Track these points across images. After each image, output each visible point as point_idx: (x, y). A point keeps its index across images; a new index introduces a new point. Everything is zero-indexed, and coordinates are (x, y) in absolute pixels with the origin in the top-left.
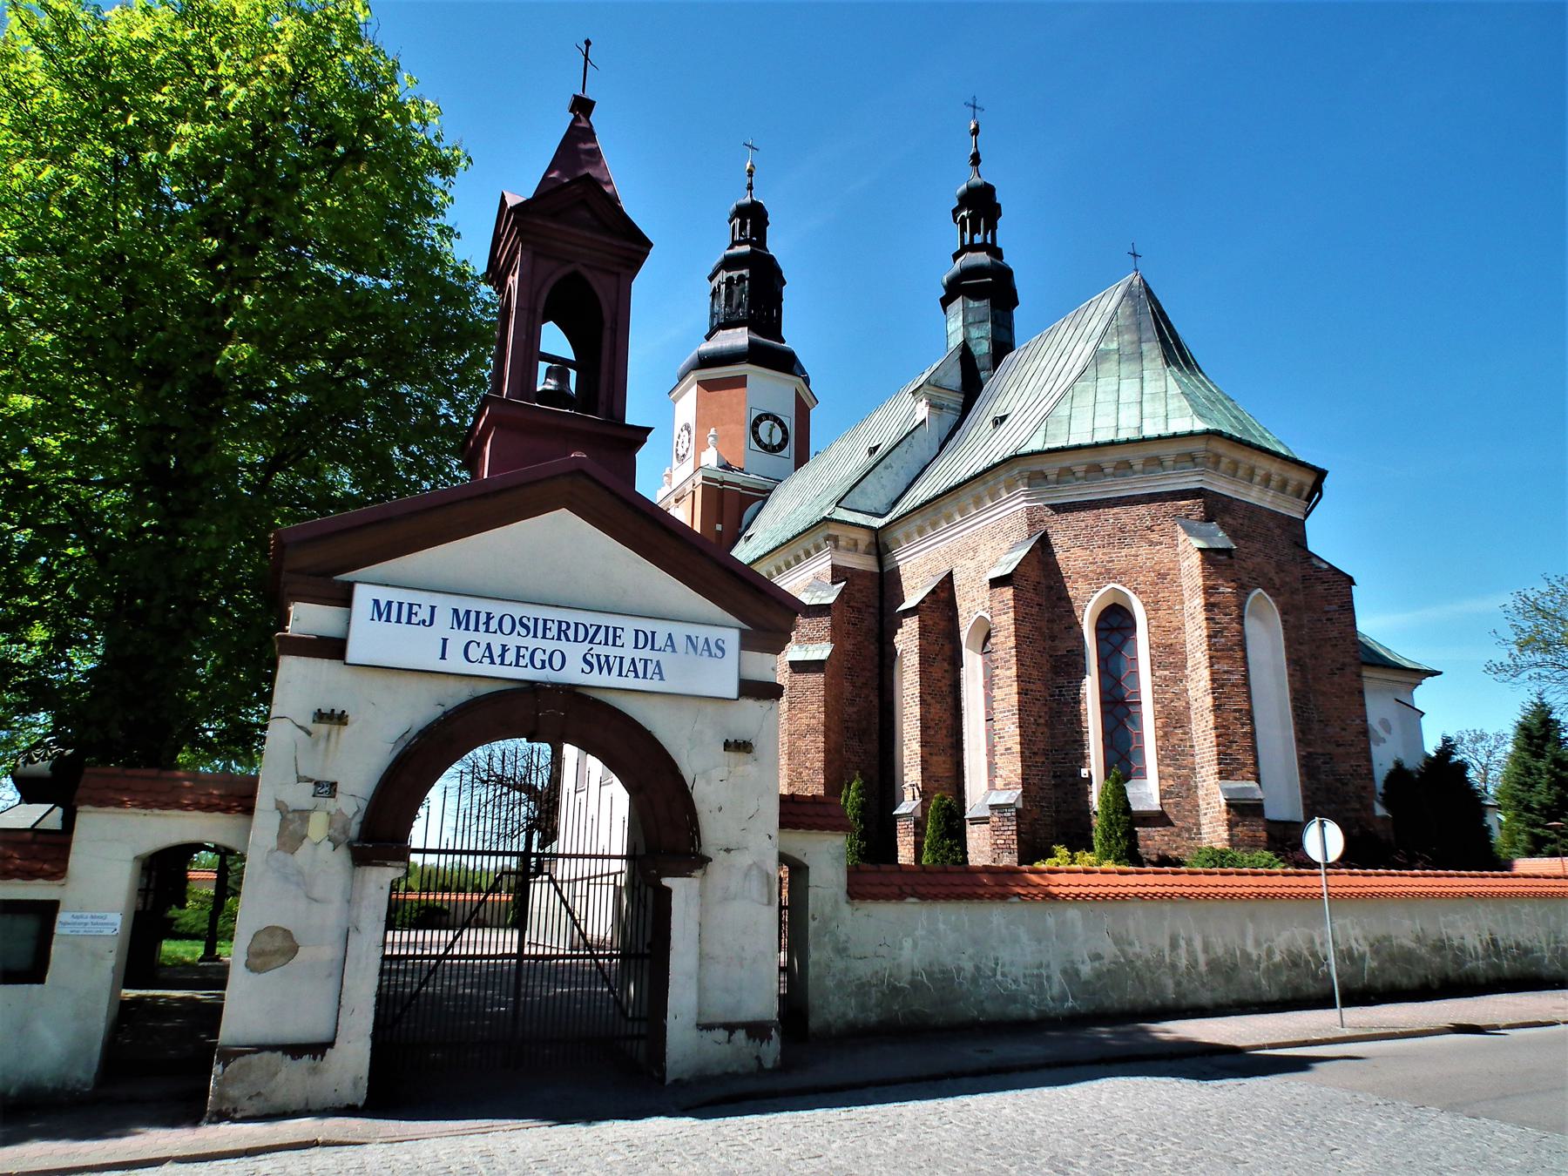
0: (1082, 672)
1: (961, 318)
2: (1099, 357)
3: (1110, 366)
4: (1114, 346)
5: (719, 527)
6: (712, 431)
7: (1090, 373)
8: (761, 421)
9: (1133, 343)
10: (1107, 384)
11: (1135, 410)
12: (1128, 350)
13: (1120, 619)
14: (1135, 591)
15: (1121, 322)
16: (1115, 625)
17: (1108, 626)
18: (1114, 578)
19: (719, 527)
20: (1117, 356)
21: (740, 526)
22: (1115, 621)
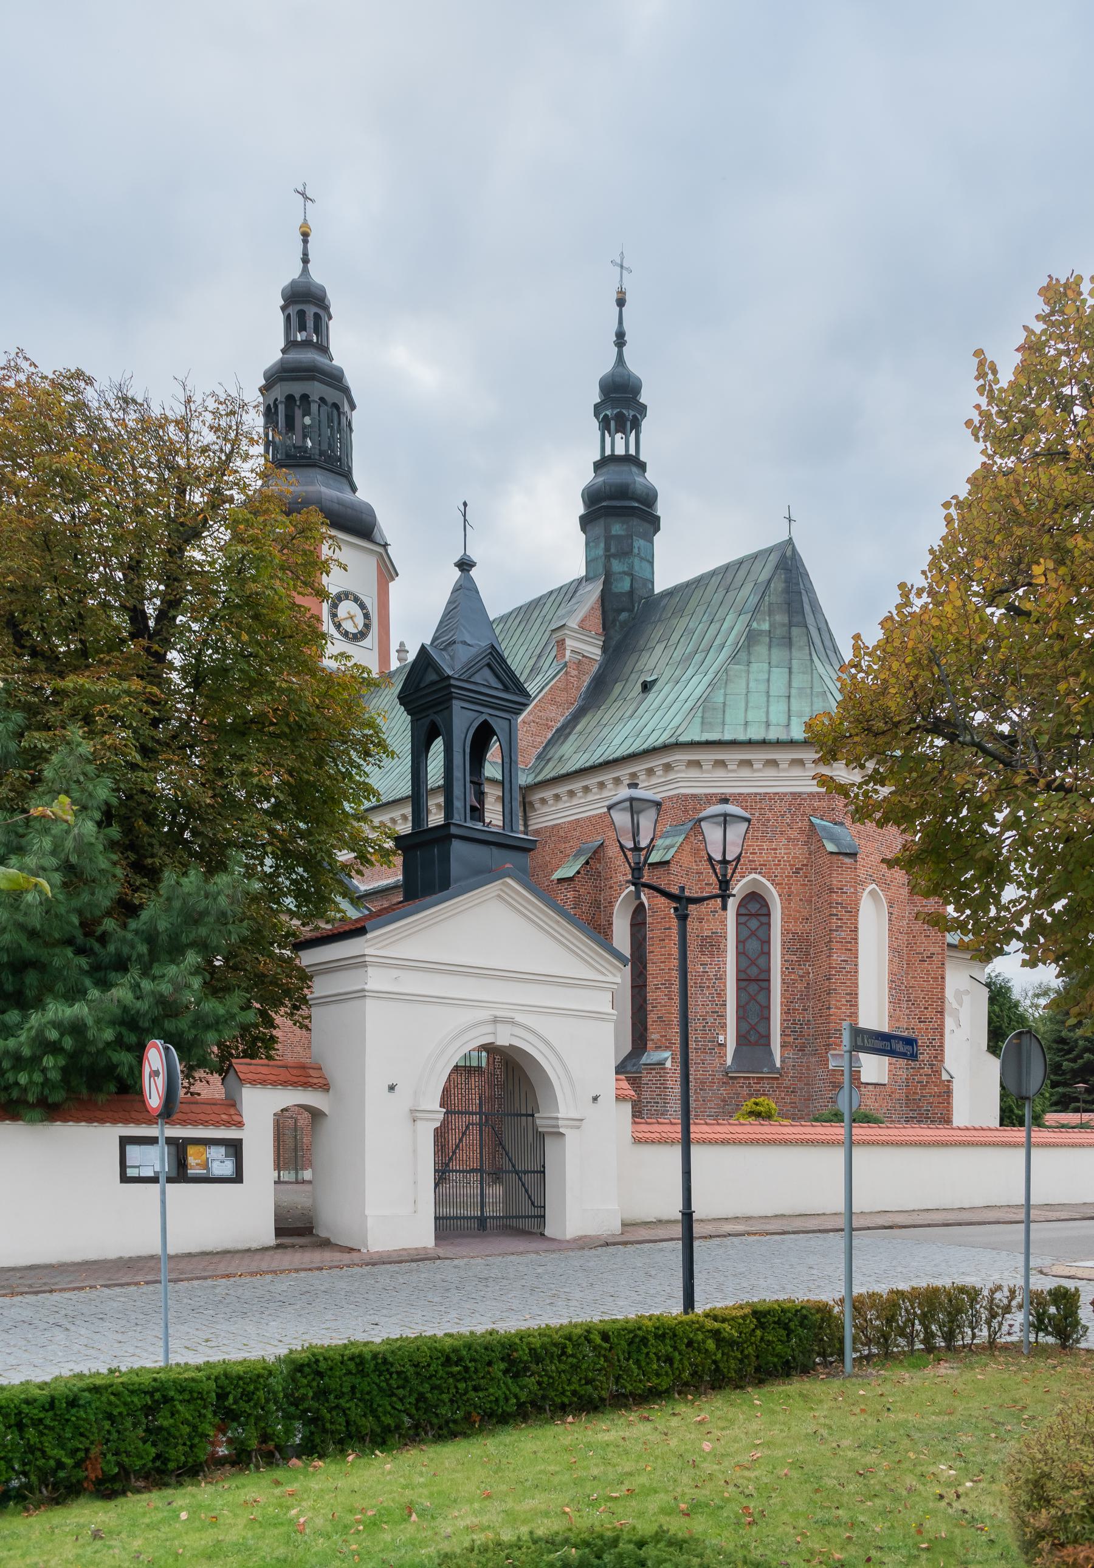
0: (722, 952)
1: (602, 545)
2: (751, 638)
3: (761, 650)
4: (766, 626)
7: (743, 655)
8: (340, 600)
9: (784, 625)
10: (758, 668)
11: (783, 706)
12: (779, 632)
13: (758, 906)
14: (773, 882)
15: (773, 599)
16: (753, 912)
17: (746, 912)
18: (754, 870)
20: (767, 639)
22: (754, 907)
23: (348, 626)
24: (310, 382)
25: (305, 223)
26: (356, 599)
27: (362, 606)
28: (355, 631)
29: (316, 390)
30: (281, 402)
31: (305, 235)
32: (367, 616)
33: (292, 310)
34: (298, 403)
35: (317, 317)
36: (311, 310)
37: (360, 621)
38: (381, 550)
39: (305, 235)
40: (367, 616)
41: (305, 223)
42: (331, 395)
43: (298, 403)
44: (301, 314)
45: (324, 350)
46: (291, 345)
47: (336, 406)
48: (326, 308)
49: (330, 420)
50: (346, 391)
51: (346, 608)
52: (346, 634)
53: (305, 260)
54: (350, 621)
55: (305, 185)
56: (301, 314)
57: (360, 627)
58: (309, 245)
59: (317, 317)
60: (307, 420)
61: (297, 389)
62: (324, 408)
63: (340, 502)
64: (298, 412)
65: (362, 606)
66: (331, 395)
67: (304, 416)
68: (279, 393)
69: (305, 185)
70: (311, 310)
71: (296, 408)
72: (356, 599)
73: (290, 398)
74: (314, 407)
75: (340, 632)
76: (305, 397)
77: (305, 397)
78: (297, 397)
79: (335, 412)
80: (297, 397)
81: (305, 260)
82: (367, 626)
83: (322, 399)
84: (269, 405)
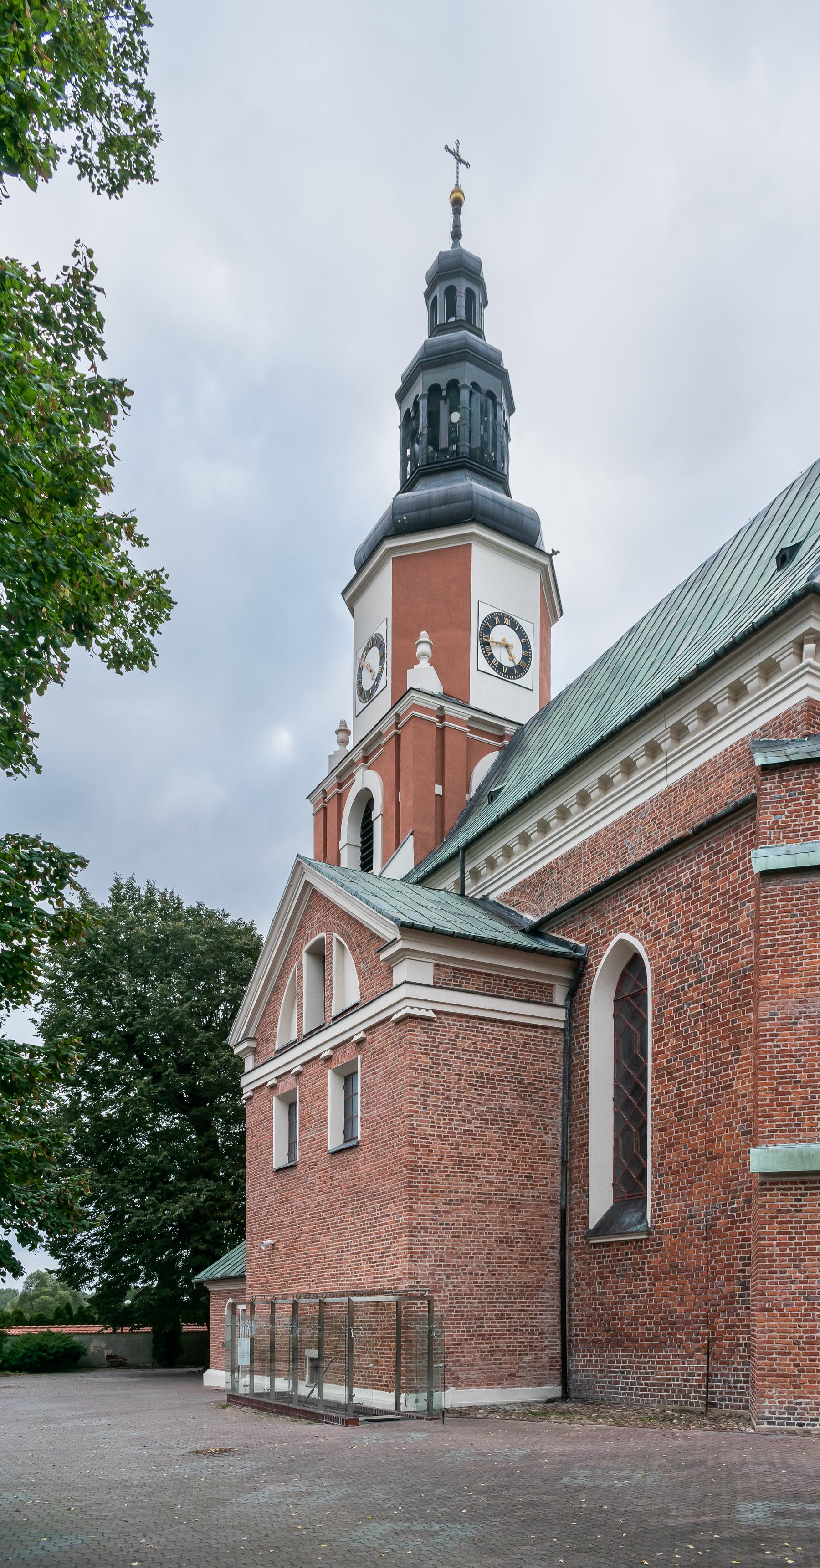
5: (438, 790)
6: (424, 635)
8: (494, 624)
19: (438, 790)
21: (468, 790)
23: (501, 656)
24: (461, 364)
25: (458, 189)
26: (514, 625)
27: (521, 633)
28: (511, 665)
29: (467, 373)
30: (423, 396)
31: (457, 204)
32: (526, 646)
33: (439, 292)
34: (444, 394)
35: (470, 295)
36: (462, 285)
37: (518, 652)
38: (546, 562)
39: (457, 204)
40: (526, 646)
41: (458, 189)
42: (486, 381)
43: (444, 394)
44: (450, 293)
45: (480, 333)
46: (435, 329)
47: (491, 395)
48: (480, 283)
49: (484, 413)
50: (503, 376)
51: (499, 633)
52: (499, 668)
53: (456, 235)
54: (504, 650)
55: (458, 143)
56: (450, 293)
57: (518, 660)
58: (462, 217)
59: (470, 295)
60: (455, 417)
61: (441, 376)
62: (477, 395)
63: (495, 500)
64: (444, 407)
65: (521, 633)
66: (486, 381)
67: (451, 412)
68: (419, 389)
69: (458, 143)
70: (462, 285)
71: (442, 403)
72: (514, 625)
73: (434, 391)
74: (465, 394)
75: (492, 666)
76: (453, 385)
77: (453, 385)
78: (443, 386)
79: (490, 403)
80: (443, 386)
81: (456, 235)
82: (526, 659)
83: (475, 385)
84: (408, 410)
